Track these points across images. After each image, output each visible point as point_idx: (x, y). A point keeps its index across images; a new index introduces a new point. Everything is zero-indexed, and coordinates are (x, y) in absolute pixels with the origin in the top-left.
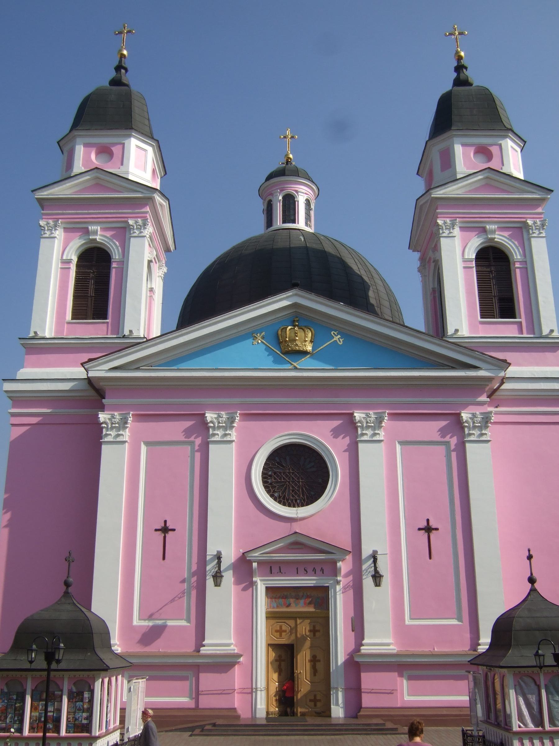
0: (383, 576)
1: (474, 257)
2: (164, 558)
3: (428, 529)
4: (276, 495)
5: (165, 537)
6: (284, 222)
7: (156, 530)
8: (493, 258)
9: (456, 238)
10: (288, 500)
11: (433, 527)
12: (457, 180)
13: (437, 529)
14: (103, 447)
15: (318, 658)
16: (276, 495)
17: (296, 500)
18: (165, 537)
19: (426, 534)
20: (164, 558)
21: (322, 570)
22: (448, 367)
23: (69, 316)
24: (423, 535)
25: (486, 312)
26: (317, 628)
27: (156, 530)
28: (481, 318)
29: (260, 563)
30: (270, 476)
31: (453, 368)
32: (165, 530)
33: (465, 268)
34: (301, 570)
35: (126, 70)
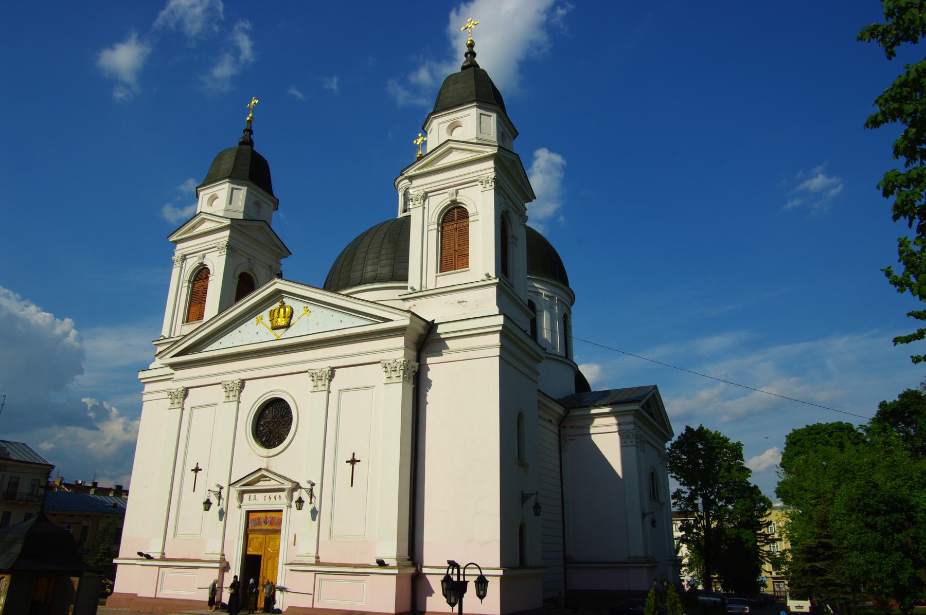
0: (304, 502)
3: (353, 462)
5: (196, 475)
11: (357, 459)
13: (359, 461)
16: (264, 440)
18: (196, 475)
19: (352, 465)
20: (194, 491)
21: (280, 497)
22: (375, 323)
24: (349, 466)
29: (244, 492)
31: (379, 323)
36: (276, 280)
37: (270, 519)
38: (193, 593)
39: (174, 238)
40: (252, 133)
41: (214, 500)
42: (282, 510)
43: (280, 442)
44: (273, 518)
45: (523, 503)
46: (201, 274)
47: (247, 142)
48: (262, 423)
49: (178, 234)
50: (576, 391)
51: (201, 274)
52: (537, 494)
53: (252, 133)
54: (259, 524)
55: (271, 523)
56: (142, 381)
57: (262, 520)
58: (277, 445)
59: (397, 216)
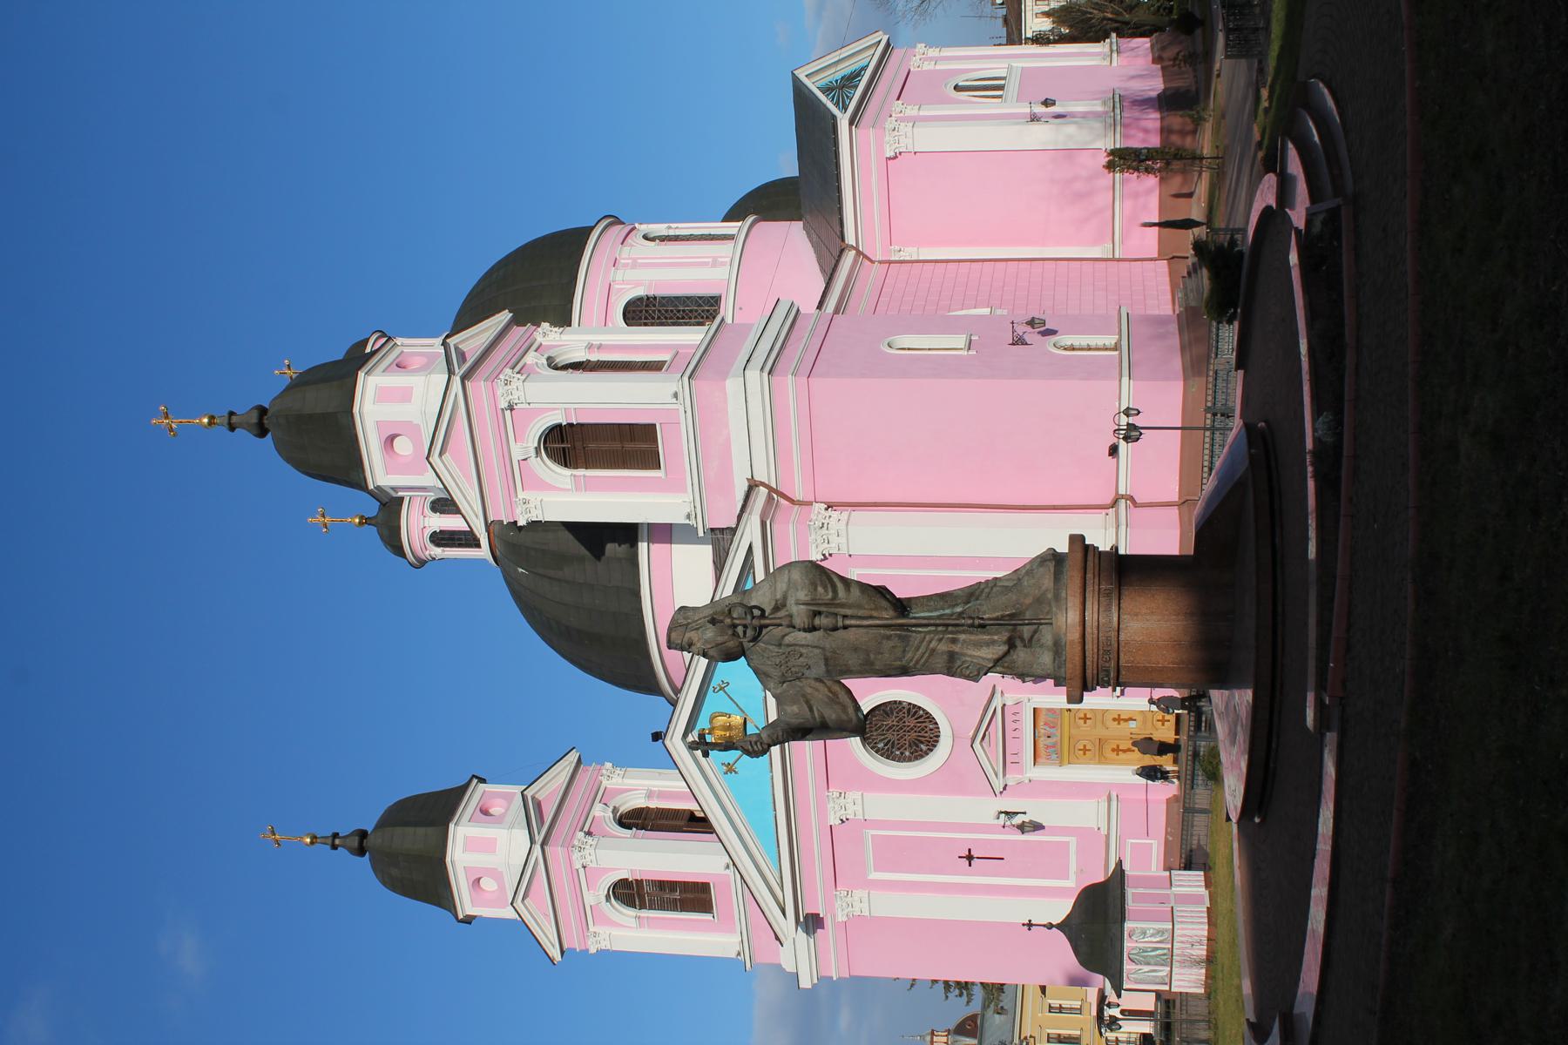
1: (567, 472)
2: (1003, 859)
4: (924, 747)
5: (978, 858)
6: (478, 545)
7: (970, 865)
8: (563, 442)
9: (544, 499)
10: (931, 738)
12: (445, 487)
14: (877, 913)
15: (1117, 717)
16: (924, 747)
17: (931, 730)
18: (978, 858)
20: (1003, 859)
23: (708, 917)
25: (650, 460)
26: (1082, 716)
27: (970, 865)
28: (659, 467)
30: (902, 753)
31: (752, 566)
32: (970, 858)
33: (586, 491)
34: (1015, 734)
35: (335, 835)
36: (667, 742)
37: (1048, 729)
38: (1154, 843)
39: (555, 953)
40: (338, 834)
41: (1018, 820)
42: (1034, 709)
43: (929, 717)
44: (1046, 724)
45: (1026, 344)
46: (629, 892)
47: (361, 843)
48: (898, 753)
49: (551, 948)
50: (800, 220)
51: (629, 892)
52: (1013, 323)
53: (338, 834)
54: (1053, 747)
55: (1053, 727)
56: (815, 981)
57: (1049, 742)
58: (936, 723)
59: (485, 560)
